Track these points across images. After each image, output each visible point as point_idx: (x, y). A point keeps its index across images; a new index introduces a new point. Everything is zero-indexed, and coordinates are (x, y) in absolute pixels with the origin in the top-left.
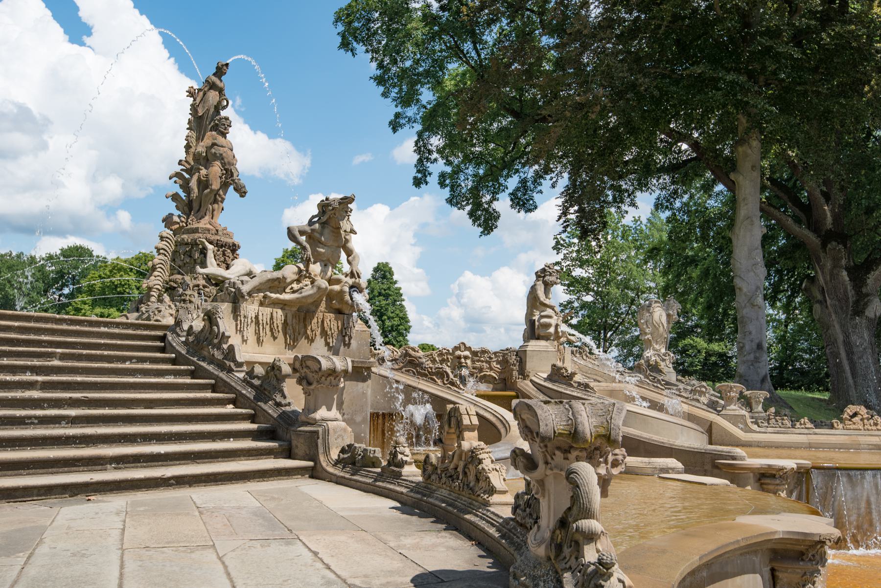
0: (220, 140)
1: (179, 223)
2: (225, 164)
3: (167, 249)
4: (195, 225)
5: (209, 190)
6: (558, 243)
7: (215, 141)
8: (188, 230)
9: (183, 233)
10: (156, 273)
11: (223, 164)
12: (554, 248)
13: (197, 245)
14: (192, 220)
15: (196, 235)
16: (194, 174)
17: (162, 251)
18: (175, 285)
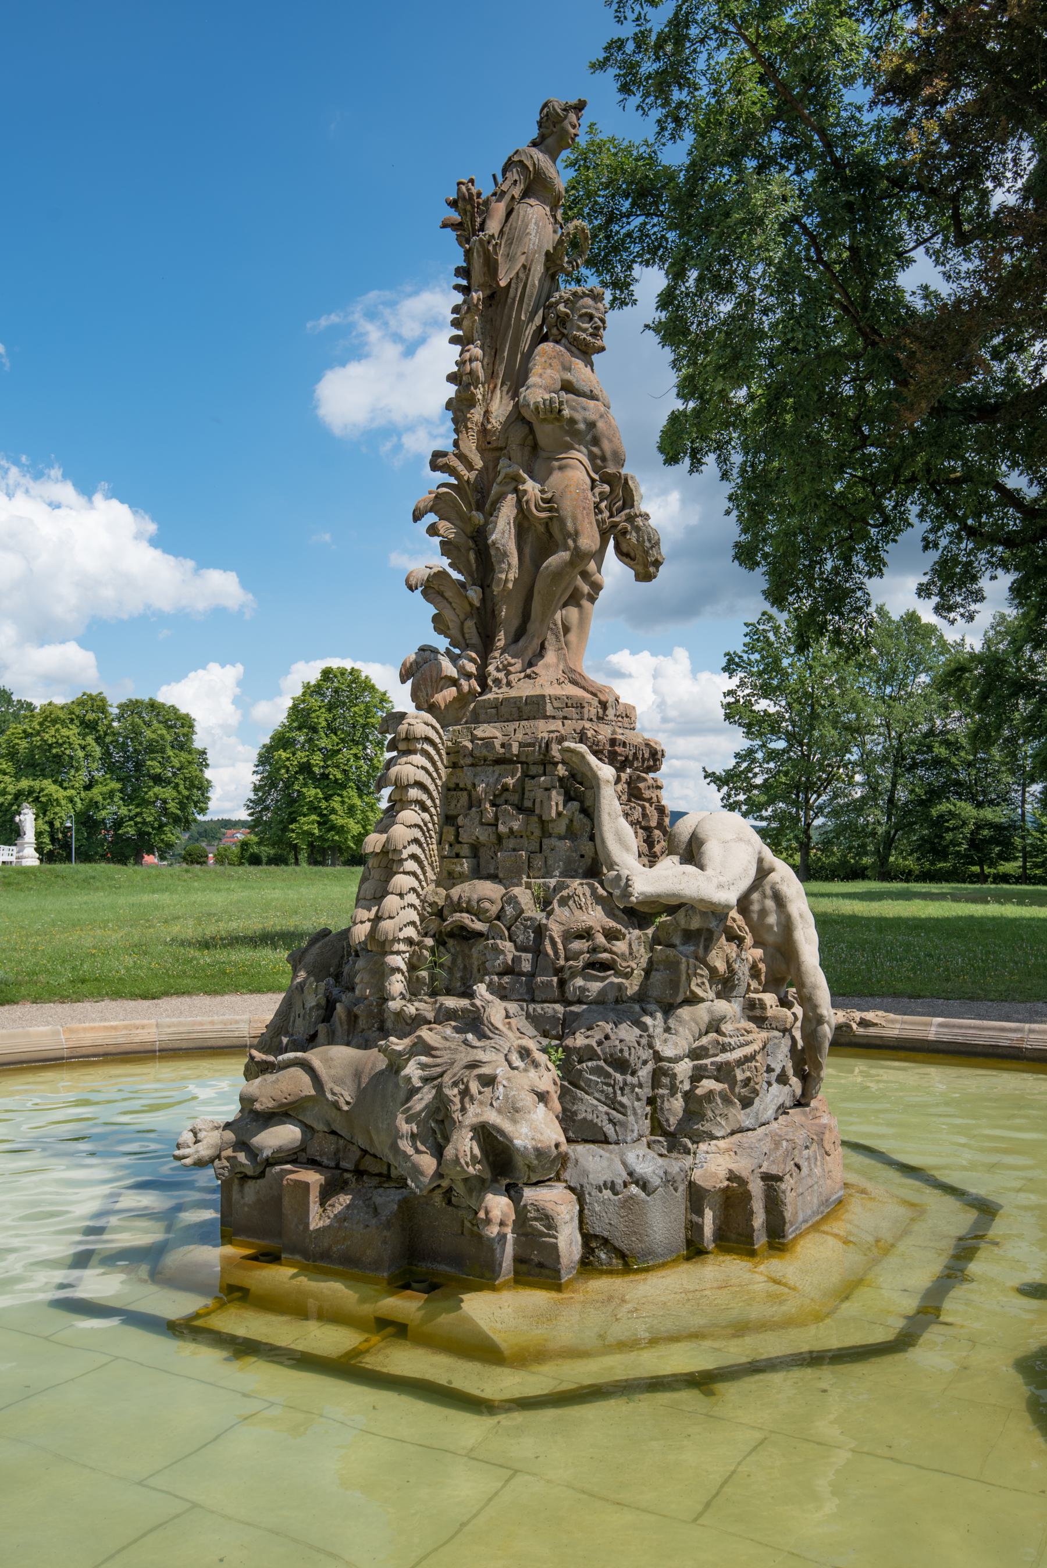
0: (581, 373)
1: (454, 682)
2: (604, 459)
3: (428, 782)
4: (524, 689)
5: (564, 555)
6: (731, 661)
7: (568, 376)
8: (497, 705)
9: (476, 719)
10: (402, 881)
11: (598, 461)
12: (725, 669)
13: (547, 762)
14: (506, 668)
15: (543, 729)
16: (501, 497)
17: (414, 793)
18: (479, 926)
